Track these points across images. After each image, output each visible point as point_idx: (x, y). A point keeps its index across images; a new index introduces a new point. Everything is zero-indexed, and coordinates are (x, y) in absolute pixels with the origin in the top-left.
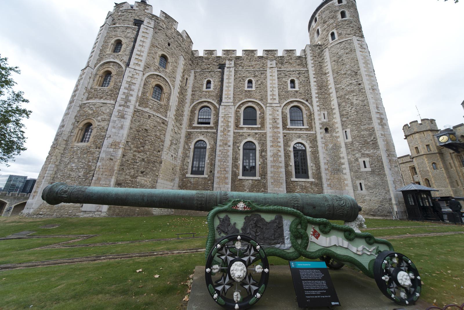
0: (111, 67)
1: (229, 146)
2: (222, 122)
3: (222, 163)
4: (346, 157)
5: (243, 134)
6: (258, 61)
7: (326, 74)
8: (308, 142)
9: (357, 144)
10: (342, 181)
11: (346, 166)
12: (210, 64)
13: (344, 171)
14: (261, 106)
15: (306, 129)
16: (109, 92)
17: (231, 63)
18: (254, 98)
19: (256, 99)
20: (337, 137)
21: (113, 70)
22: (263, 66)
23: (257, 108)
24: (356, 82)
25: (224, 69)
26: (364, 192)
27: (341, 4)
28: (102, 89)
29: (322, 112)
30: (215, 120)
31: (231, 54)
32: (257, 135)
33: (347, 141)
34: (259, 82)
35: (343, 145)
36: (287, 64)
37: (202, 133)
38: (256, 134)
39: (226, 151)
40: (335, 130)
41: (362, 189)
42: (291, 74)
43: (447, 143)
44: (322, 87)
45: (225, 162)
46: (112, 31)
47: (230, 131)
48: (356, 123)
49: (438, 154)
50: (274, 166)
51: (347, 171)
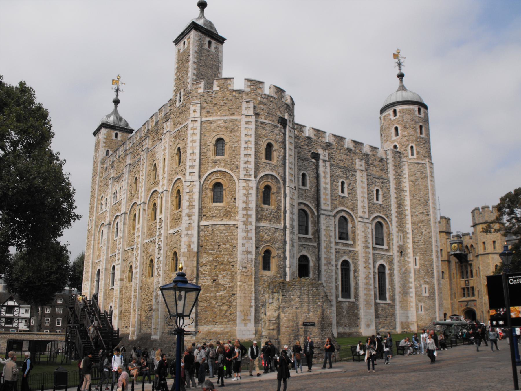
0: (270, 180)
1: (332, 266)
2: (325, 235)
3: (328, 284)
4: (413, 283)
5: (340, 250)
6: (347, 155)
7: (403, 191)
8: (388, 264)
9: (422, 272)
10: (409, 303)
11: (413, 290)
12: (302, 147)
13: (411, 295)
14: (352, 217)
15: (386, 250)
16: (275, 214)
17: (325, 153)
18: (347, 207)
19: (349, 209)
20: (409, 262)
21: (270, 182)
22: (352, 164)
23: (349, 219)
24: (427, 212)
25: (319, 160)
26: (423, 312)
27: (420, 116)
28: (269, 209)
29: (399, 234)
30: (313, 230)
31: (321, 137)
32: (351, 253)
33: (416, 267)
34: (350, 187)
35: (412, 271)
36: (372, 165)
37: (304, 246)
38: (350, 251)
39: (330, 271)
40: (407, 254)
41: (421, 311)
42: (376, 182)
43: (456, 252)
44: (400, 205)
45: (330, 283)
46: (261, 128)
47: (332, 247)
48: (423, 253)
49: (447, 262)
50: (366, 288)
51: (413, 295)
